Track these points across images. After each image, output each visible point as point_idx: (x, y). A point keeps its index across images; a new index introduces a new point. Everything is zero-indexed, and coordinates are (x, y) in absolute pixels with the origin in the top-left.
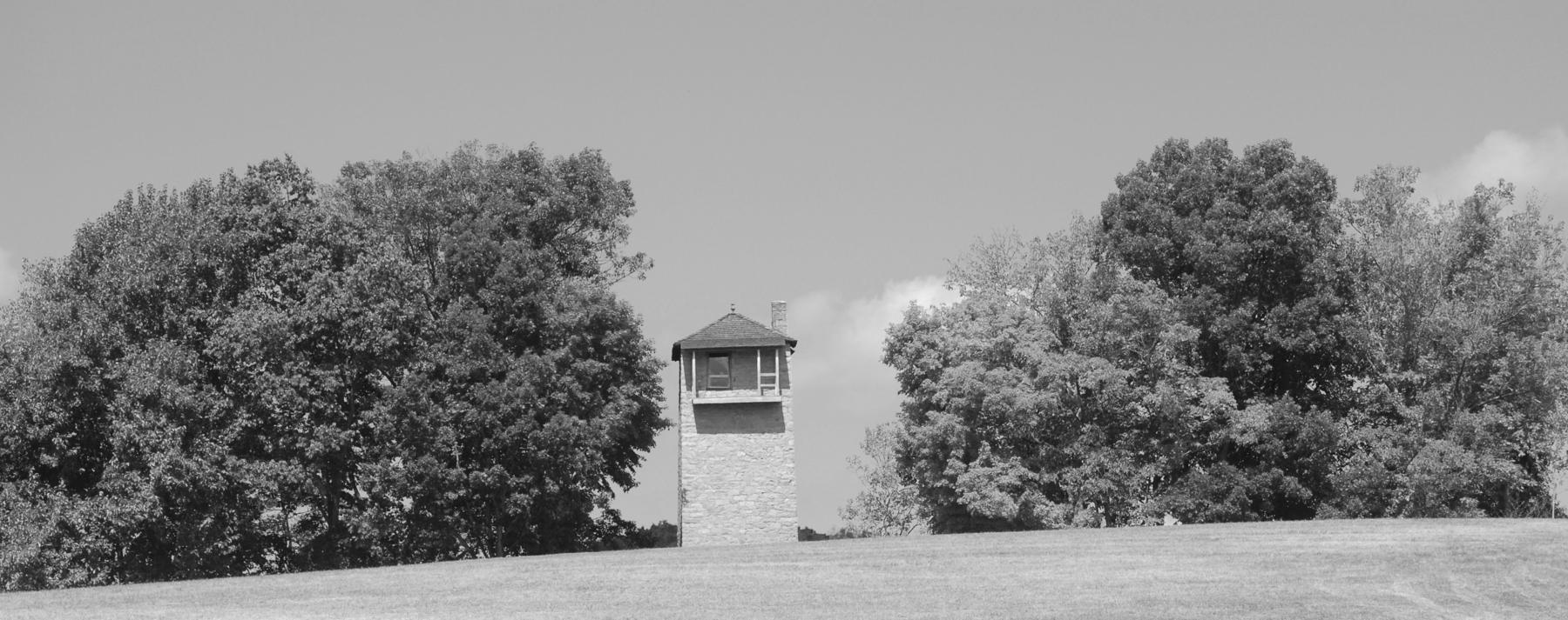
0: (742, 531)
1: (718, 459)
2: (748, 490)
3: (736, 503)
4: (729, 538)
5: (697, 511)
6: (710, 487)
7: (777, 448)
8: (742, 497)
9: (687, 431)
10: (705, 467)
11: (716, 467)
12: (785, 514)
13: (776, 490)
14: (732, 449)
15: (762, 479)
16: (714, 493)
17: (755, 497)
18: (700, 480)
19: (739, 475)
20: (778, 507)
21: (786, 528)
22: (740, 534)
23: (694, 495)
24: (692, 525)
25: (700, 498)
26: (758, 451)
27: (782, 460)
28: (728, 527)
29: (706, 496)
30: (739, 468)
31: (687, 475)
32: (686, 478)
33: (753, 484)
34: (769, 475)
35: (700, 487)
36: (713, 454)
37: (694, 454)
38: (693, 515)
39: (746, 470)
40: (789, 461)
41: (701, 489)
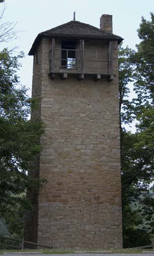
0: (82, 171)
5: (50, 155)
6: (60, 138)
7: (108, 113)
8: (83, 147)
9: (45, 97)
10: (57, 123)
14: (77, 112)
15: (98, 134)
18: (53, 133)
21: (112, 170)
22: (81, 173)
24: (47, 165)
25: (53, 146)
30: (81, 126)
33: (91, 137)
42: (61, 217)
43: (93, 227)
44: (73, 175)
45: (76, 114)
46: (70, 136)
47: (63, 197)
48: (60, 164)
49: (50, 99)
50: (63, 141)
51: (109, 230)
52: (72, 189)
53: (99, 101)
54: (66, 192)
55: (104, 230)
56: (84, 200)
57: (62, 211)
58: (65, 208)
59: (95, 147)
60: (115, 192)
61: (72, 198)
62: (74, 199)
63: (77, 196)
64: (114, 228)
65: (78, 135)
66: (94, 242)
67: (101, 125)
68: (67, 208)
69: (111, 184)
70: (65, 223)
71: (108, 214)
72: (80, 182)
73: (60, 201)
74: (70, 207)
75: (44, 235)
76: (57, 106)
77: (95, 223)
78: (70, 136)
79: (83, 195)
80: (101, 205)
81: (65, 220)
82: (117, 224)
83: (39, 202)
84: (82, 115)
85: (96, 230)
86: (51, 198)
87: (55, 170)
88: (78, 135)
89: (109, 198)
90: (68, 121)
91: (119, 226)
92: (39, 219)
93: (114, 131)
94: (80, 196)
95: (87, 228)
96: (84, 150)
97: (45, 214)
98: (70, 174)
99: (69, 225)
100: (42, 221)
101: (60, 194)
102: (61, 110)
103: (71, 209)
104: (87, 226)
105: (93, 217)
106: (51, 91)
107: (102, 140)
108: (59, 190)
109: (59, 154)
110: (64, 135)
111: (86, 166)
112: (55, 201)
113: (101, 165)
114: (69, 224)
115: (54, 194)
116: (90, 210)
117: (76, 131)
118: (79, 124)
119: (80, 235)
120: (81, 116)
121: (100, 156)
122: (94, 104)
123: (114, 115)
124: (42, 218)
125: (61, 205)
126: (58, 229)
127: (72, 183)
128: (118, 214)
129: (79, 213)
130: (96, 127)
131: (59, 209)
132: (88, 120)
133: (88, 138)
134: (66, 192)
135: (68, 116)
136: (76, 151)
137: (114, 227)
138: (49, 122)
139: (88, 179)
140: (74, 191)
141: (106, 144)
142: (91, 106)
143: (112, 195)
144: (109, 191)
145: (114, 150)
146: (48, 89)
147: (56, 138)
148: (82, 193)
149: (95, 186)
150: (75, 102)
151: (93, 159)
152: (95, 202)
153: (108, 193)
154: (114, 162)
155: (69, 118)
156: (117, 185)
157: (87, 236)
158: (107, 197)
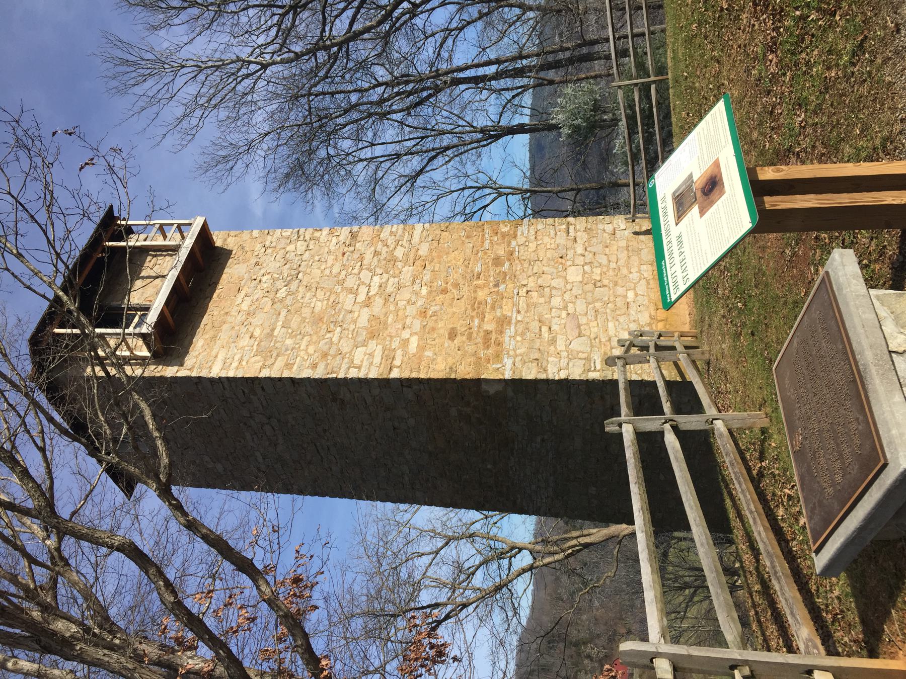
0: (424, 291)
2: (351, 282)
5: (371, 355)
6: (329, 335)
7: (291, 248)
18: (311, 350)
25: (345, 349)
42: (545, 329)
47: (489, 326)
55: (580, 250)
56: (502, 287)
59: (368, 269)
64: (576, 231)
67: (317, 258)
68: (519, 318)
72: (453, 293)
73: (501, 332)
75: (598, 367)
76: (245, 341)
87: (415, 345)
95: (574, 275)
100: (555, 370)
101: (482, 334)
109: (372, 337)
112: (499, 344)
114: (564, 314)
125: (510, 331)
126: (580, 335)
129: (535, 294)
131: (523, 334)
134: (476, 321)
135: (277, 320)
142: (264, 279)
149: (467, 267)
152: (507, 265)
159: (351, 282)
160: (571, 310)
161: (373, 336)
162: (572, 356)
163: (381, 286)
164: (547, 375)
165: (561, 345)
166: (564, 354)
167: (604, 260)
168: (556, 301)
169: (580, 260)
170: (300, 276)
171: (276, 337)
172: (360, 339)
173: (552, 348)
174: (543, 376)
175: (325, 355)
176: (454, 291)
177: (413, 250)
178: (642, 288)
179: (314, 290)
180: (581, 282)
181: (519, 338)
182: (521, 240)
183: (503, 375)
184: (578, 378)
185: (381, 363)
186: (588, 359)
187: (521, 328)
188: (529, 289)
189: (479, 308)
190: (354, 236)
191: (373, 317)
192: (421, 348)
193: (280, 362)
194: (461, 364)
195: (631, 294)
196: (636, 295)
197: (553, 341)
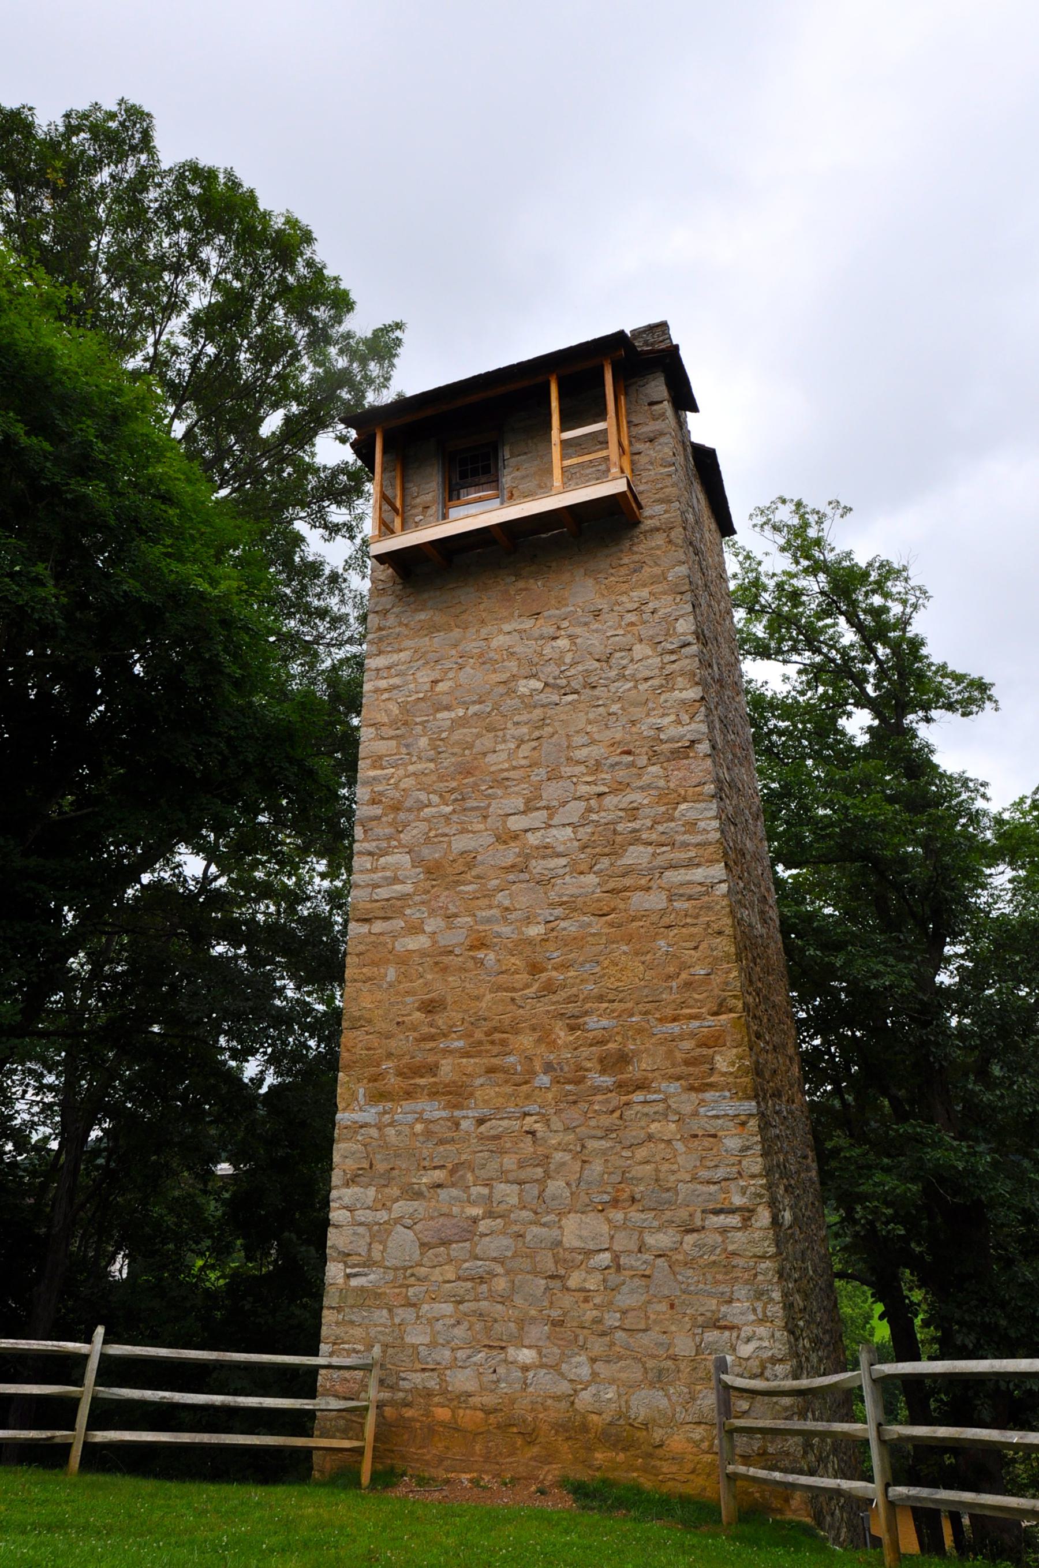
0: (535, 931)
1: (461, 712)
2: (552, 792)
3: (515, 837)
4: (490, 957)
5: (396, 880)
6: (435, 798)
7: (640, 650)
10: (423, 742)
11: (457, 736)
12: (683, 855)
13: (646, 779)
14: (504, 677)
15: (596, 752)
16: (447, 818)
17: (574, 810)
18: (408, 783)
19: (525, 750)
20: (654, 837)
21: (687, 905)
22: (529, 942)
23: (388, 831)
24: (378, 927)
26: (580, 668)
27: (656, 682)
28: (488, 920)
29: (423, 826)
30: (525, 730)
31: (372, 773)
32: (367, 783)
33: (567, 770)
34: (618, 736)
35: (408, 804)
36: (445, 700)
37: (396, 710)
38: (383, 893)
39: (549, 730)
40: (680, 681)
41: (410, 810)
42: (439, 1175)
43: (605, 1228)
44: (492, 956)
45: (502, 689)
46: (475, 786)
47: (447, 1068)
48: (432, 912)
49: (395, 657)
50: (449, 809)
51: (690, 1239)
52: (486, 1026)
53: (597, 614)
54: (459, 1044)
56: (545, 1080)
57: (442, 1142)
58: (457, 1125)
59: (589, 810)
60: (711, 1020)
61: (491, 1070)
62: (500, 1076)
63: (512, 1059)
64: (724, 1231)
65: (511, 774)
66: (612, 1319)
67: (615, 708)
68: (465, 1124)
69: (684, 976)
70: (455, 1210)
71: (679, 1146)
72: (527, 986)
73: (433, 1094)
74: (481, 1122)
75: (354, 1282)
76: (425, 677)
77: (615, 1203)
78: (475, 786)
79: (543, 1048)
80: (638, 1097)
81: (454, 1192)
82: (738, 1201)
83: (341, 1105)
84: (525, 687)
85: (616, 1248)
86: (393, 1081)
87: (410, 947)
88: (511, 774)
89: (679, 1056)
90: (463, 726)
91: (747, 1213)
92: (334, 1194)
93: (678, 722)
94: (529, 1059)
96: (539, 834)
97: (366, 1165)
98: (481, 955)
99: (475, 1220)
100: (346, 1201)
101: (431, 1059)
102: (441, 687)
103: (482, 1128)
104: (571, 1222)
105: (597, 1167)
106: (400, 624)
107: (621, 774)
108: (432, 1038)
109: (428, 872)
110: (454, 784)
111: (552, 905)
112: (409, 1095)
113: (626, 889)
114: (476, 1211)
115: (406, 1060)
116: (582, 1131)
117: (504, 756)
118: (518, 723)
119: (535, 1272)
120: (522, 690)
121: (615, 850)
122: (578, 631)
123: (672, 652)
124: (347, 1185)
125: (435, 1110)
127: (489, 997)
128: (733, 1143)
129: (527, 1146)
130: (589, 722)
131: (428, 1133)
132: (555, 698)
133: (553, 776)
135: (466, 705)
136: (505, 842)
137: (721, 1220)
138: (394, 743)
139: (564, 966)
140: (497, 1036)
141: (642, 788)
142: (563, 643)
143: (693, 1035)
144: (675, 1020)
145: (683, 806)
146: (391, 620)
147: (418, 801)
148: (539, 1041)
149: (601, 999)
150: (494, 644)
151: (583, 867)
152: (607, 1080)
153: (675, 1028)
154: (691, 864)
155: (474, 709)
156: (717, 980)
157: (572, 1283)
158: (670, 1052)
159: (552, 792)
160: (483, 1226)
161: (433, 871)
162: (379, 1233)
163: (546, 848)
164: (337, 1187)
165: (401, 1208)
166: (383, 1216)
167: (624, 1300)
168: (507, 1193)
169: (623, 1242)
170: (570, 698)
171: (435, 719)
172: (426, 852)
173: (395, 1192)
174: (337, 1177)
175: (396, 808)
176: (536, 986)
177: (643, 882)
178: (544, 1382)
179: (537, 734)
180: (560, 1243)
181: (419, 1127)
182: (687, 1103)
183: (344, 1110)
184: (329, 1243)
185: (377, 901)
186: (369, 1263)
187: (442, 1130)
188: (539, 1135)
189: (492, 1043)
190: (686, 750)
191: (470, 859)
192: (403, 960)
193: (383, 747)
194: (368, 1033)
195: (527, 1356)
196: (525, 1369)
197: (418, 1195)
